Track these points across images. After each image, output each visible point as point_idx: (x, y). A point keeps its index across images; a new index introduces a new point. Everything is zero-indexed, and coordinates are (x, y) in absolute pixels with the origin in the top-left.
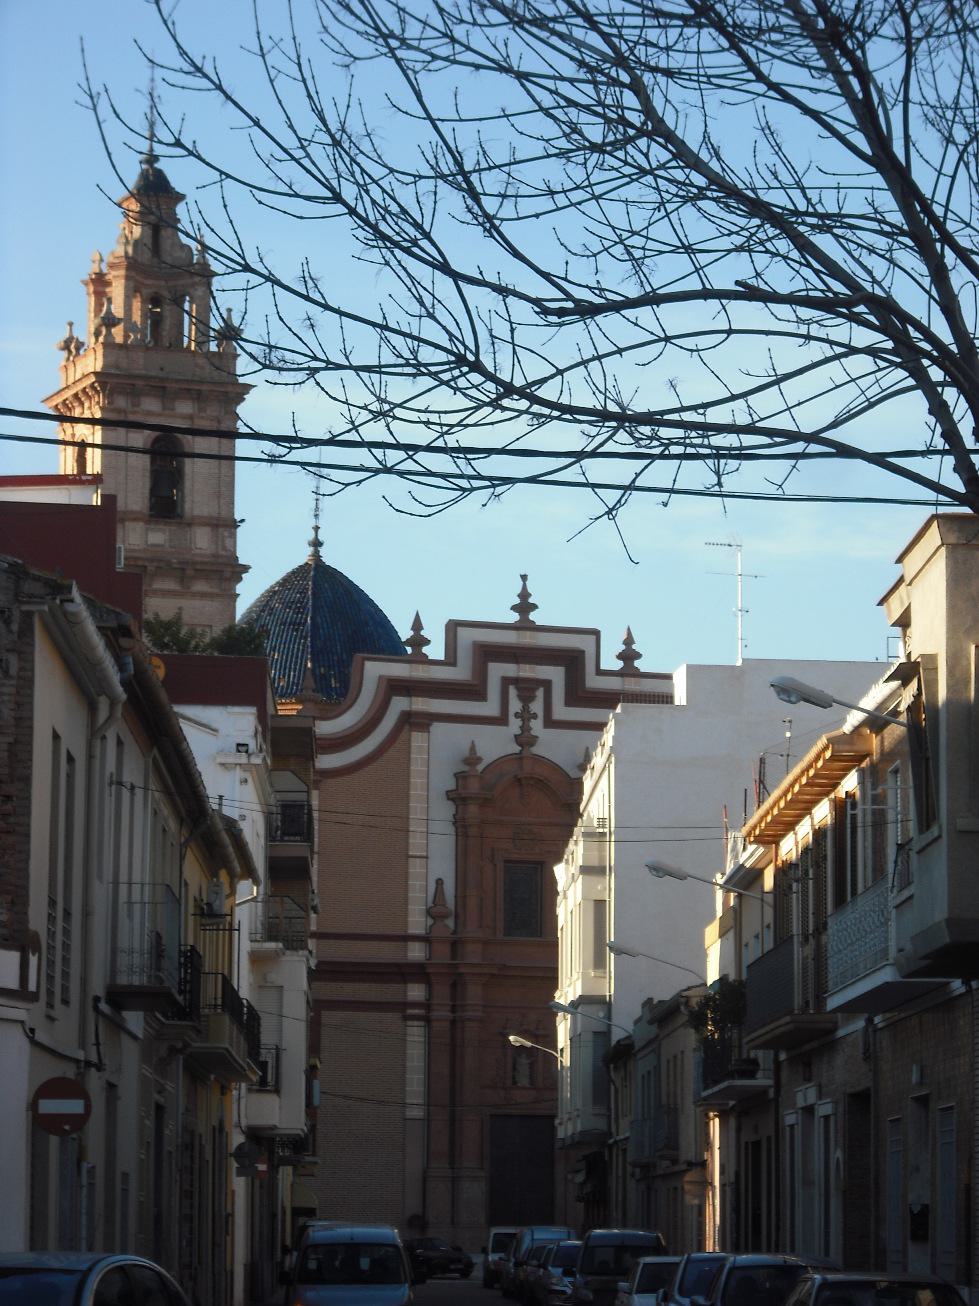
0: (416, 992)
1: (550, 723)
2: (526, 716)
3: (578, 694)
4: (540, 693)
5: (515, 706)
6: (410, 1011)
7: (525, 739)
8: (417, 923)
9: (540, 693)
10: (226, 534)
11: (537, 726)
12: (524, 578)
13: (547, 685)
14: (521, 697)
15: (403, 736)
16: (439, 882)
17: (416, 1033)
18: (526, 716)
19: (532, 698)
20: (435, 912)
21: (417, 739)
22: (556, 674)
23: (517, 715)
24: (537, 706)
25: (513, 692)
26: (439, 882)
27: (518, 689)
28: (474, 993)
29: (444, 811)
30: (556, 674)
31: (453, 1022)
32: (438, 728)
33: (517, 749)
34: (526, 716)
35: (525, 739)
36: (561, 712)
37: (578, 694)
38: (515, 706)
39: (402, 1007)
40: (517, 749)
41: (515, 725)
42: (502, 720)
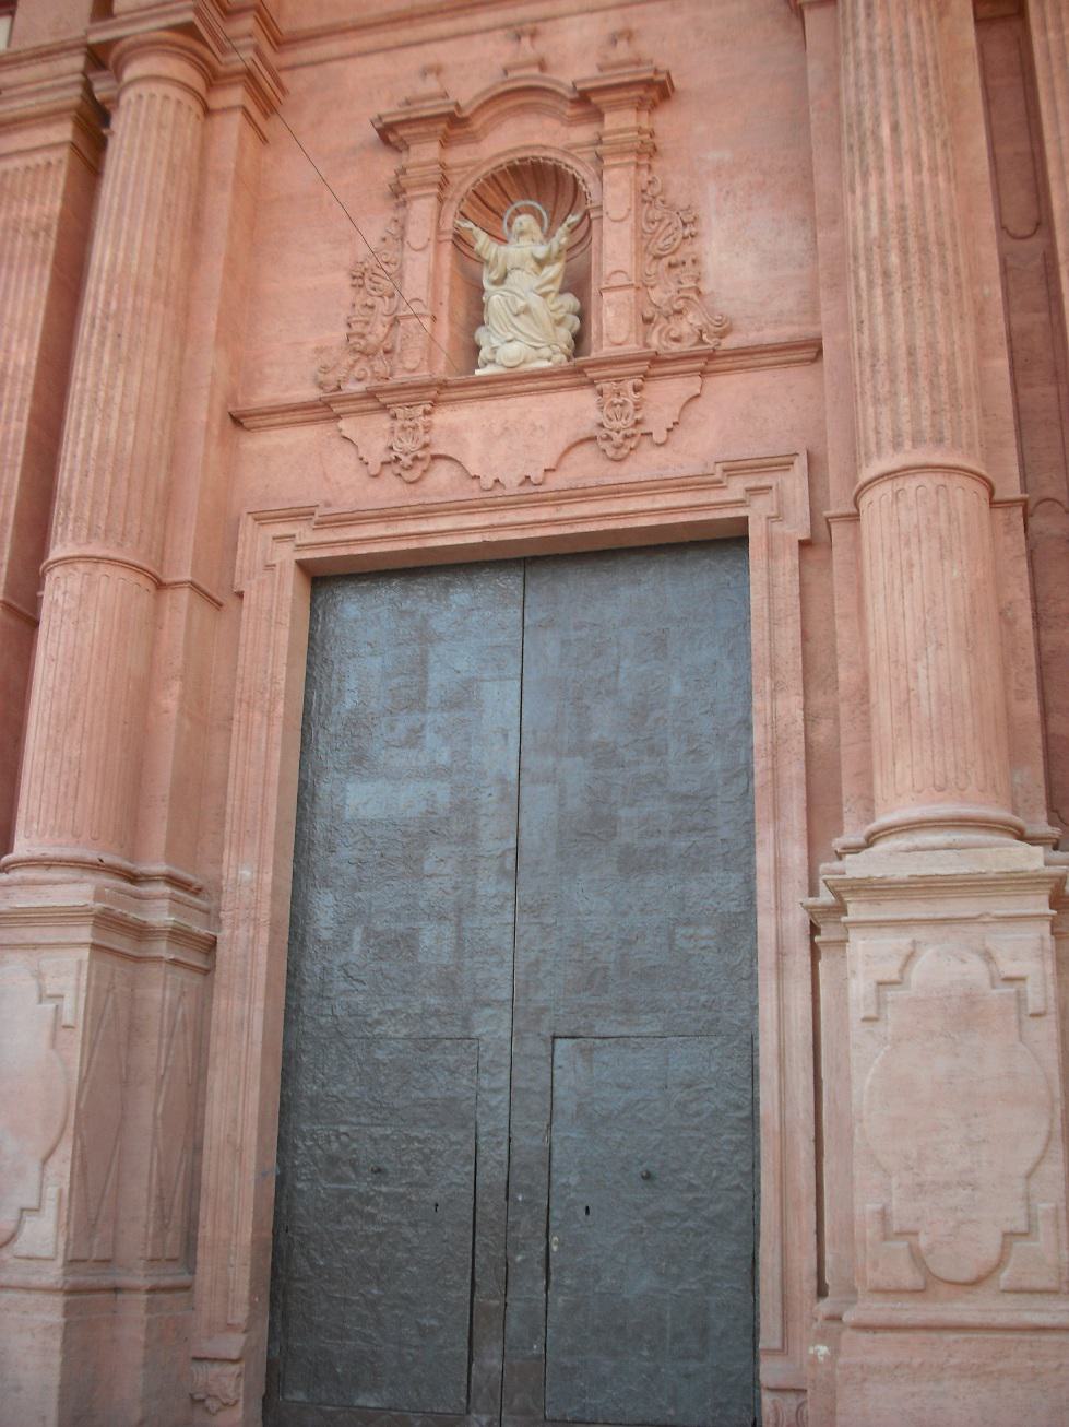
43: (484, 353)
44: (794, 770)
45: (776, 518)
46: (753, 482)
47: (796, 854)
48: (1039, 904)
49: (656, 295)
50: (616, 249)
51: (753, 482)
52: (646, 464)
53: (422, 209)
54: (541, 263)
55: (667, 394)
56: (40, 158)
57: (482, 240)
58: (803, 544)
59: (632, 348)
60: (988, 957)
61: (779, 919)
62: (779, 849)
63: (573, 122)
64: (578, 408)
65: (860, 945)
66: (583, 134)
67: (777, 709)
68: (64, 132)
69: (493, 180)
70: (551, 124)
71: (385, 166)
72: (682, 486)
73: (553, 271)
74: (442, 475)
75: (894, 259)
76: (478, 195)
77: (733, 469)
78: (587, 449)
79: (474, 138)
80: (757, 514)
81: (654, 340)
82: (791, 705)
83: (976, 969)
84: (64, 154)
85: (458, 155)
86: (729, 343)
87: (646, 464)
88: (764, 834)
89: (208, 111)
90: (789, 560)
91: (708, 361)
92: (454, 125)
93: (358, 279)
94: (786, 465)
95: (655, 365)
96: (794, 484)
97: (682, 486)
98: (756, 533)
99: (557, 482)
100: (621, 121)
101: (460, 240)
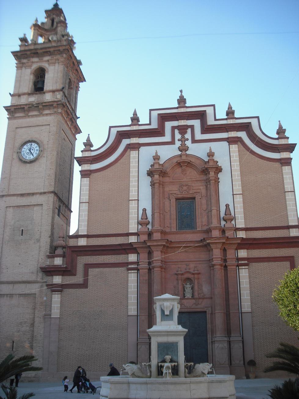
0: (133, 258)
1: (194, 141)
2: (183, 139)
3: (206, 129)
4: (189, 131)
5: (178, 136)
6: (130, 266)
7: (183, 149)
8: (133, 227)
9: (189, 131)
10: (58, 93)
11: (188, 143)
12: (181, 91)
13: (192, 127)
14: (180, 133)
15: (127, 153)
16: (144, 210)
17: (133, 277)
18: (183, 140)
19: (186, 132)
20: (143, 222)
21: (133, 154)
22: (196, 123)
23: (179, 140)
24: (188, 135)
25: (176, 131)
26: (144, 210)
27: (178, 130)
28: (157, 256)
29: (146, 181)
30: (196, 123)
31: (150, 270)
32: (142, 149)
33: (180, 153)
34: (183, 140)
35: (183, 149)
36: (199, 136)
37: (206, 129)
38: (178, 136)
39: (126, 264)
40: (180, 153)
41: (178, 144)
42: (172, 142)
43: (185, 295)
44: (210, 330)
45: (209, 311)
46: (207, 308)
47: (210, 336)
48: (226, 342)
49: (199, 292)
50: (196, 288)
51: (207, 308)
52: (199, 306)
53: (180, 282)
54: (190, 287)
55: (201, 300)
56: (145, 273)
57: (185, 285)
58: (211, 314)
59: (198, 297)
60: (223, 345)
61: (209, 341)
62: (209, 336)
63: (192, 275)
64: (194, 301)
65: (216, 344)
66: (192, 276)
67: (209, 326)
68: (147, 271)
69: (185, 279)
70: (190, 275)
71: (176, 276)
72: (201, 308)
73: (191, 288)
74: (183, 306)
75: (218, 296)
76: (184, 280)
77: (205, 307)
78: (194, 305)
79: (184, 275)
80: (207, 311)
81: (199, 296)
82: (210, 326)
83: (223, 346)
84: (147, 273)
85: (182, 276)
86: (205, 297)
87: (199, 306)
88: (208, 335)
89: (161, 271)
90: (210, 315)
91: (203, 299)
92: (182, 274)
93: (175, 287)
94: (209, 307)
95: (200, 298)
96: (210, 309)
97: (201, 308)
98: (207, 312)
99: (192, 307)
100: (196, 276)
101: (183, 285)
